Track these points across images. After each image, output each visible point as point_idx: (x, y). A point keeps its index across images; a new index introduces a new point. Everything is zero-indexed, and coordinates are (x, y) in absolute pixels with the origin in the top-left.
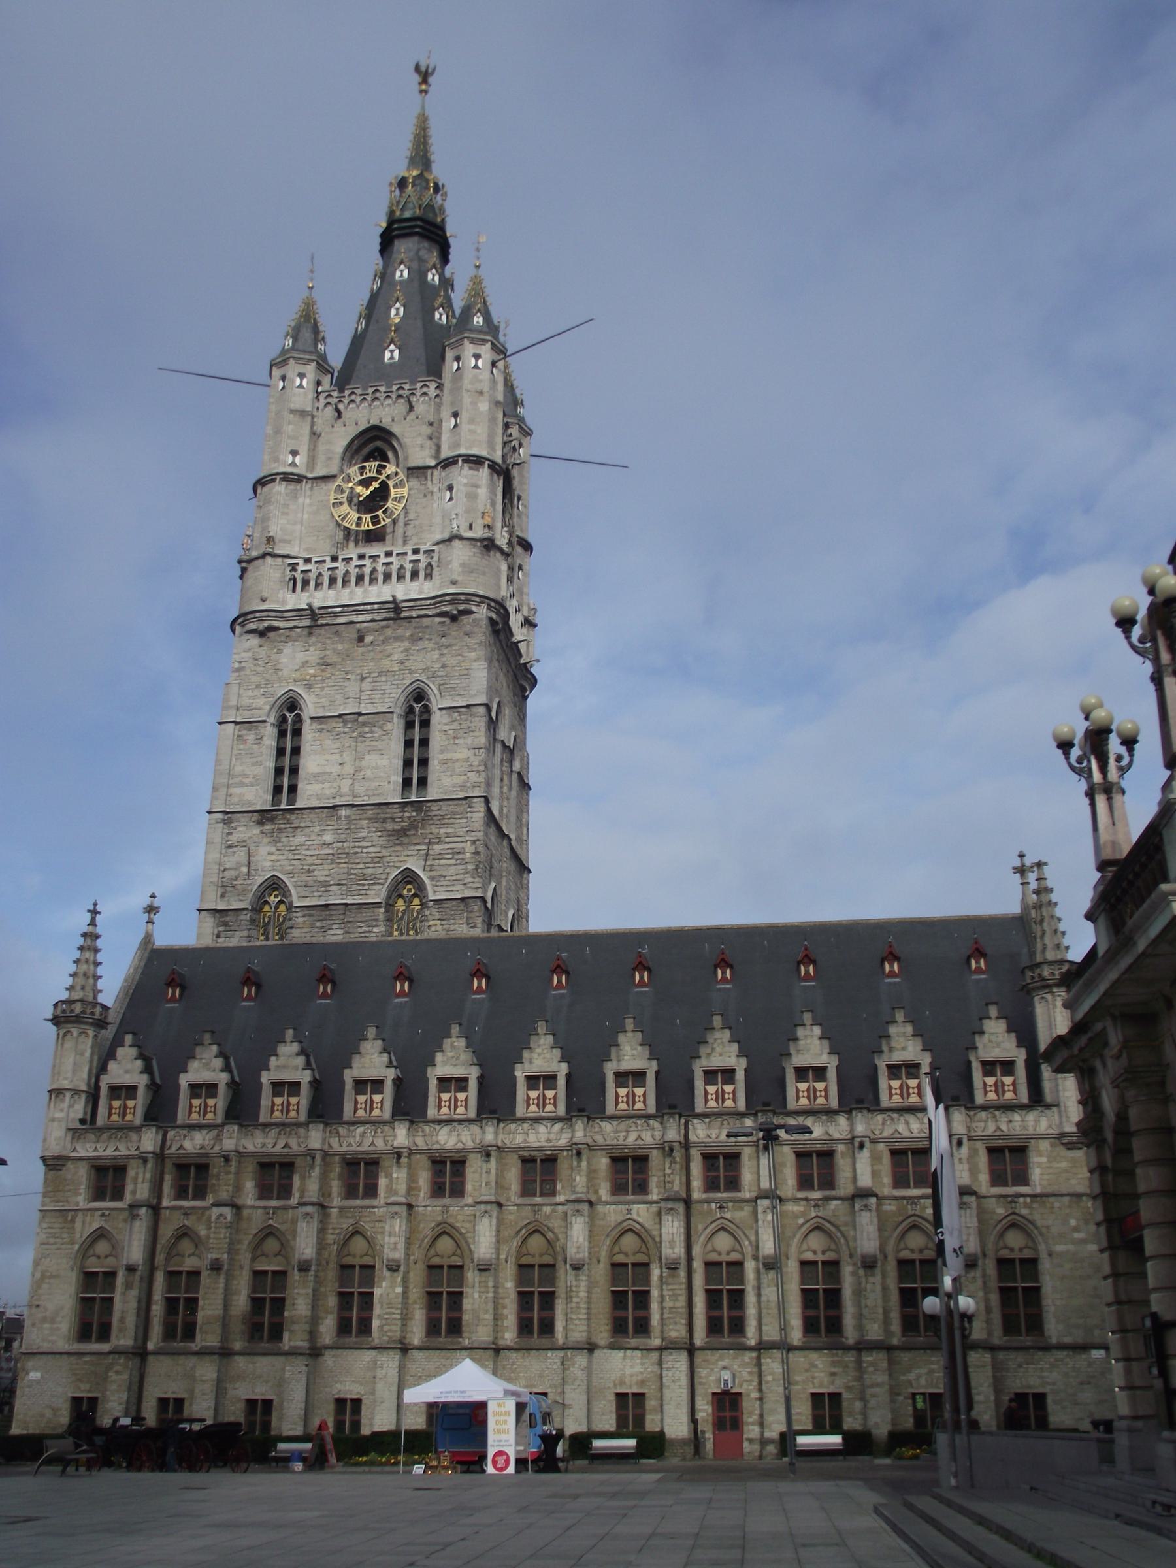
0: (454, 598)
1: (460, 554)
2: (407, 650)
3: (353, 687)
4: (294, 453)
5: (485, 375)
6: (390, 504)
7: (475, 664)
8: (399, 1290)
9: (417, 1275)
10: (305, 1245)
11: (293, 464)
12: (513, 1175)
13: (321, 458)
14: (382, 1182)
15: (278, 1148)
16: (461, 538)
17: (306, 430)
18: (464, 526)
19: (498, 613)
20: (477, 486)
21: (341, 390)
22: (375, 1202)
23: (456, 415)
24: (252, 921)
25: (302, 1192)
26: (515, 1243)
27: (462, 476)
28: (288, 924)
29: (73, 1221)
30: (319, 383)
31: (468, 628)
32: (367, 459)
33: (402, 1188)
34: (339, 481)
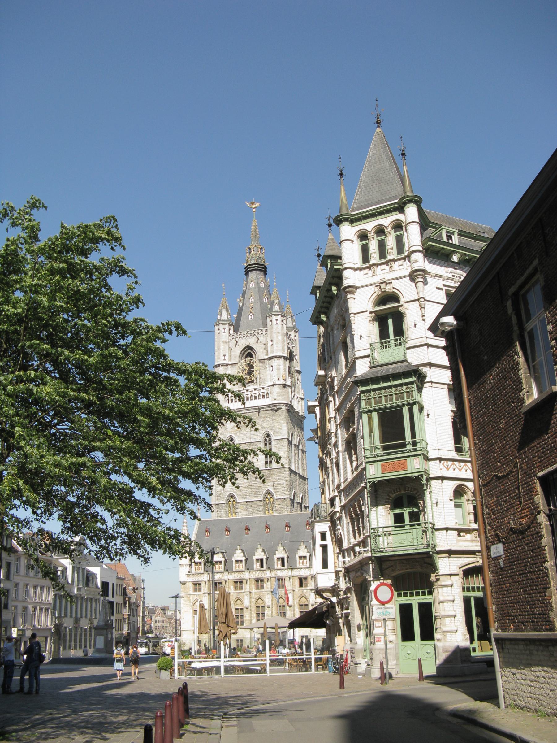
0: (275, 405)
1: (276, 389)
2: (263, 421)
3: (248, 434)
4: (224, 356)
5: (280, 326)
6: (254, 373)
7: (283, 425)
8: (270, 612)
9: (275, 608)
10: (247, 602)
11: (225, 360)
12: (297, 582)
13: (233, 357)
14: (265, 585)
15: (238, 578)
16: (276, 385)
17: (227, 347)
18: (277, 379)
19: (289, 407)
20: (280, 366)
21: (237, 334)
22: (263, 590)
23: (272, 341)
24: (226, 507)
25: (245, 588)
26: (298, 600)
27: (275, 362)
28: (236, 507)
29: (189, 597)
30: (230, 330)
31: (280, 413)
32: (246, 357)
33: (269, 587)
34: (239, 365)
